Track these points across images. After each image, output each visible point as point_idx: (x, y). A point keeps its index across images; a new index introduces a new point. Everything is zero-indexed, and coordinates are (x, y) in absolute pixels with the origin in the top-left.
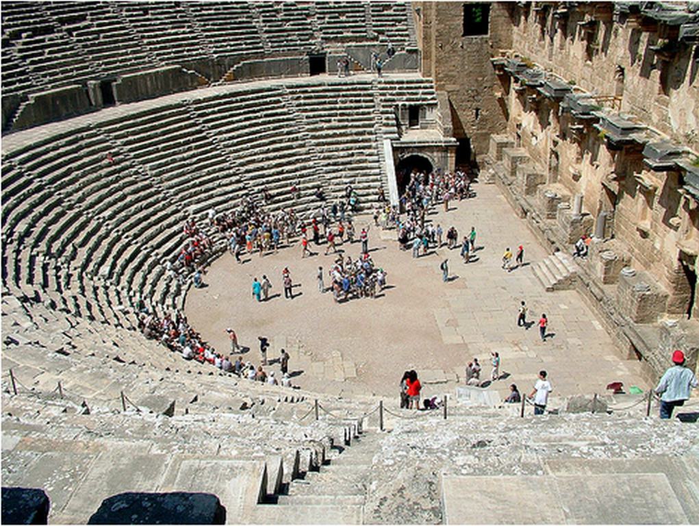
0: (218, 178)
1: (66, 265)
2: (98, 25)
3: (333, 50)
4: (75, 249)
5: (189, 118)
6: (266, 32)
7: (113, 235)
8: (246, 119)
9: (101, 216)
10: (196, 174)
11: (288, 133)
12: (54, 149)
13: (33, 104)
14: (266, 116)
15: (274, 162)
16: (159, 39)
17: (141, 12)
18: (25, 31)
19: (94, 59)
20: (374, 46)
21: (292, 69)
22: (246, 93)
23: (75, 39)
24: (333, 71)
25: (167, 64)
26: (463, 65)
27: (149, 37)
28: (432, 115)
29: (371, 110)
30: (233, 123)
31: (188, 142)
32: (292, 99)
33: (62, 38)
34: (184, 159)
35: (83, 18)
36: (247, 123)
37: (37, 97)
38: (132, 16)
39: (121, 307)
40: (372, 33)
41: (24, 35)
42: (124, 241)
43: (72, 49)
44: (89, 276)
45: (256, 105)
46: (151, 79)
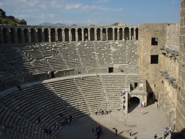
0: (77, 99)
1: (26, 119)
2: (54, 58)
3: (116, 66)
5: (73, 83)
6: (98, 61)
8: (88, 84)
10: (72, 98)
11: (99, 88)
14: (94, 83)
15: (94, 96)
16: (70, 62)
17: (66, 55)
18: (35, 58)
19: (51, 66)
20: (127, 66)
21: (103, 71)
22: (91, 77)
23: (47, 61)
24: (115, 73)
25: (70, 68)
26: (151, 72)
27: (67, 61)
28: (141, 85)
30: (85, 84)
31: (71, 89)
32: (102, 79)
33: (45, 60)
34: (69, 93)
35: (51, 56)
36: (88, 85)
38: (64, 56)
41: (35, 59)
42: (46, 114)
43: (47, 63)
45: (92, 80)
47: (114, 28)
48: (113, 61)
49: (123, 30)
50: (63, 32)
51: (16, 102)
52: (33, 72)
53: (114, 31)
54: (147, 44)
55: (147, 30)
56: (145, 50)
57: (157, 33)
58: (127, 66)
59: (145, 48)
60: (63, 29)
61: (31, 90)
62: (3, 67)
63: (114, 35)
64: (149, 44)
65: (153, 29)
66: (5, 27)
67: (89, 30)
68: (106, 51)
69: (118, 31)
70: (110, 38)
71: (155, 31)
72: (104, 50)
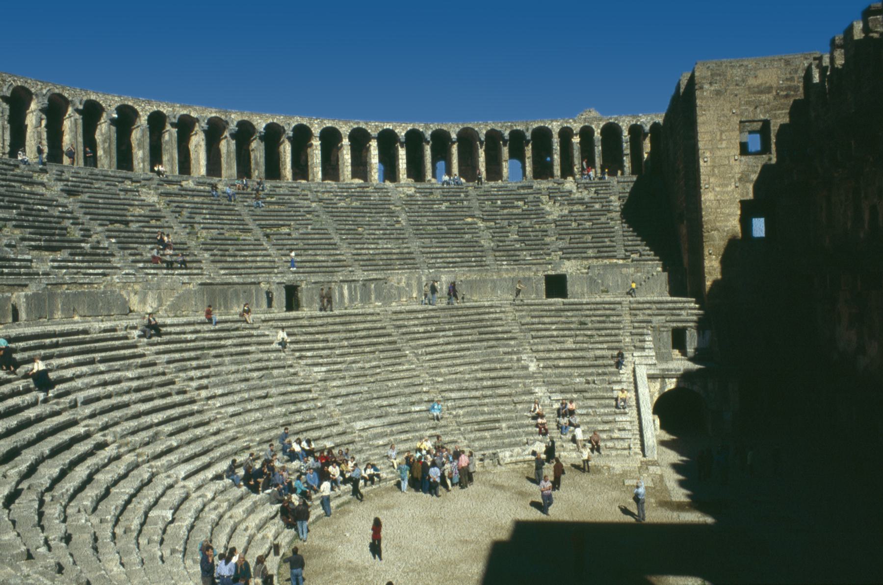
7: (231, 433)
9: (223, 411)
29: (621, 332)
37: (202, 284)
40: (621, 252)
46: (350, 288)
47: (555, 127)
48: (561, 249)
49: (597, 134)
52: (202, 274)
53: (556, 140)
54: (719, 153)
55: (716, 87)
56: (712, 180)
57: (764, 97)
60: (345, 129)
65: (743, 81)
68: (525, 215)
69: (576, 140)
70: (543, 170)
71: (755, 93)
72: (516, 211)
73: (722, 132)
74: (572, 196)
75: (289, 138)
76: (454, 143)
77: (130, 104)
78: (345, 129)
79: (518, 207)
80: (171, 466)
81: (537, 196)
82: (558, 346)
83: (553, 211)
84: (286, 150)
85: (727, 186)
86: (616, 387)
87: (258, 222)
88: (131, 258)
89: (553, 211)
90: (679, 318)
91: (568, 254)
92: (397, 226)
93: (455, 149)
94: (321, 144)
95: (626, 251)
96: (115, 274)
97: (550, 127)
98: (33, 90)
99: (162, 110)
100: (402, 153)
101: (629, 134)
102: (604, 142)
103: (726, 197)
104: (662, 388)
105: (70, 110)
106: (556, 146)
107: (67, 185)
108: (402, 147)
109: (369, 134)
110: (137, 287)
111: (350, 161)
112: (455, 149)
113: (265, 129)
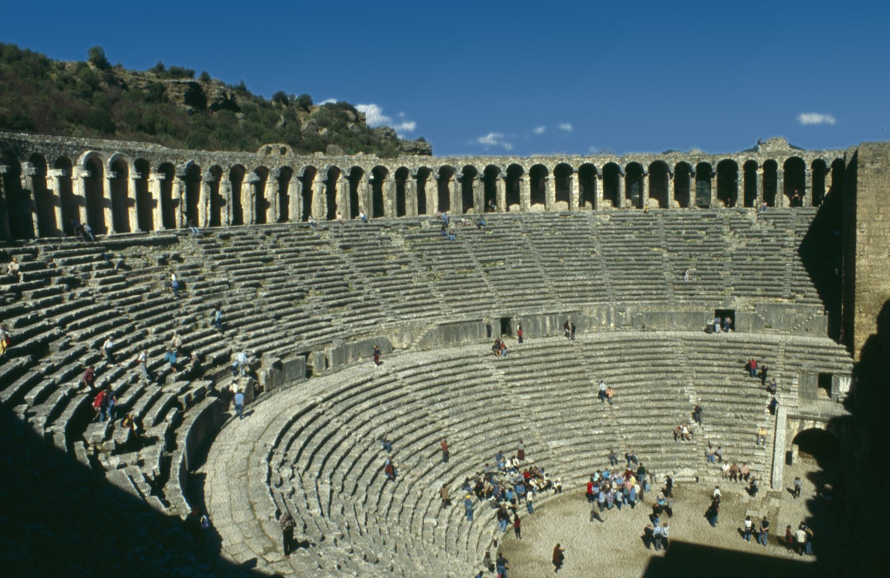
4: (419, 462)
9: (460, 435)
12: (439, 370)
13: (436, 330)
20: (790, 307)
37: (441, 325)
39: (434, 522)
40: (787, 292)
44: (422, 487)
47: (741, 160)
49: (780, 168)
50: (527, 179)
51: (374, 411)
52: (440, 315)
53: (741, 172)
55: (877, 166)
56: (866, 248)
58: (790, 307)
59: (869, 237)
60: (551, 166)
61: (426, 376)
62: (343, 294)
63: (741, 188)
64: (883, 221)
66: (356, 164)
67: (646, 169)
68: (703, 248)
69: (760, 172)
72: (699, 242)
73: (879, 206)
74: (752, 228)
75: (504, 178)
76: (646, 175)
77: (382, 164)
78: (551, 166)
79: (699, 238)
80: (431, 483)
81: (719, 226)
82: (717, 382)
83: (733, 243)
84: (501, 186)
85: (879, 254)
86: (759, 424)
87: (479, 259)
88: (391, 306)
89: (733, 243)
90: (826, 364)
91: (740, 290)
92: (593, 256)
93: (646, 180)
94: (531, 180)
95: (792, 291)
96: (382, 322)
97: (736, 160)
98: (317, 167)
99: (405, 165)
100: (600, 184)
101: (812, 167)
102: (787, 175)
103: (879, 264)
104: (801, 426)
105: (341, 176)
106: (741, 178)
107: (342, 241)
108: (600, 178)
109: (571, 169)
110: (397, 331)
111: (554, 193)
112: (646, 180)
113: (485, 172)
